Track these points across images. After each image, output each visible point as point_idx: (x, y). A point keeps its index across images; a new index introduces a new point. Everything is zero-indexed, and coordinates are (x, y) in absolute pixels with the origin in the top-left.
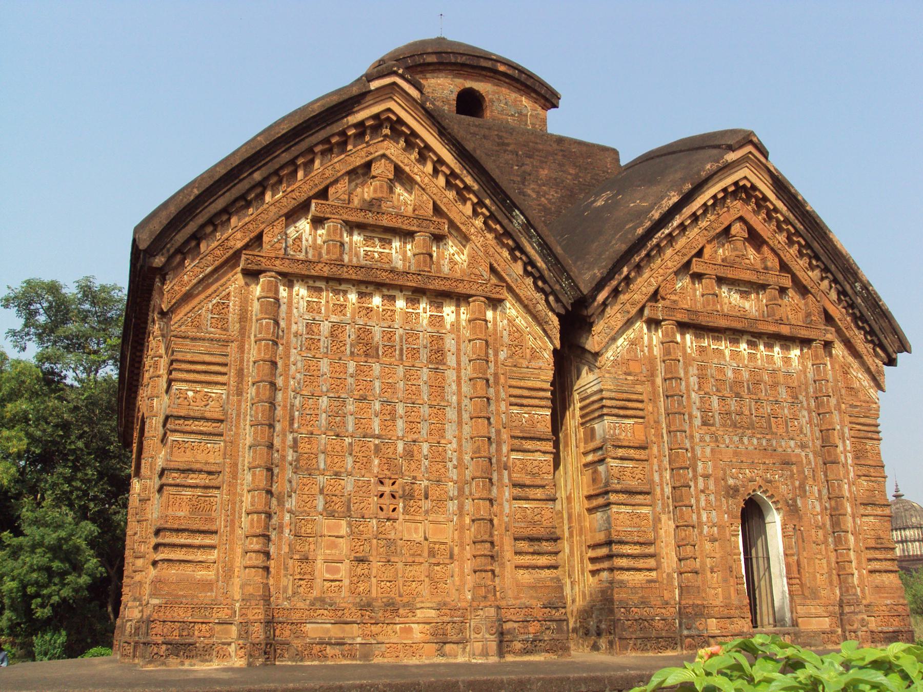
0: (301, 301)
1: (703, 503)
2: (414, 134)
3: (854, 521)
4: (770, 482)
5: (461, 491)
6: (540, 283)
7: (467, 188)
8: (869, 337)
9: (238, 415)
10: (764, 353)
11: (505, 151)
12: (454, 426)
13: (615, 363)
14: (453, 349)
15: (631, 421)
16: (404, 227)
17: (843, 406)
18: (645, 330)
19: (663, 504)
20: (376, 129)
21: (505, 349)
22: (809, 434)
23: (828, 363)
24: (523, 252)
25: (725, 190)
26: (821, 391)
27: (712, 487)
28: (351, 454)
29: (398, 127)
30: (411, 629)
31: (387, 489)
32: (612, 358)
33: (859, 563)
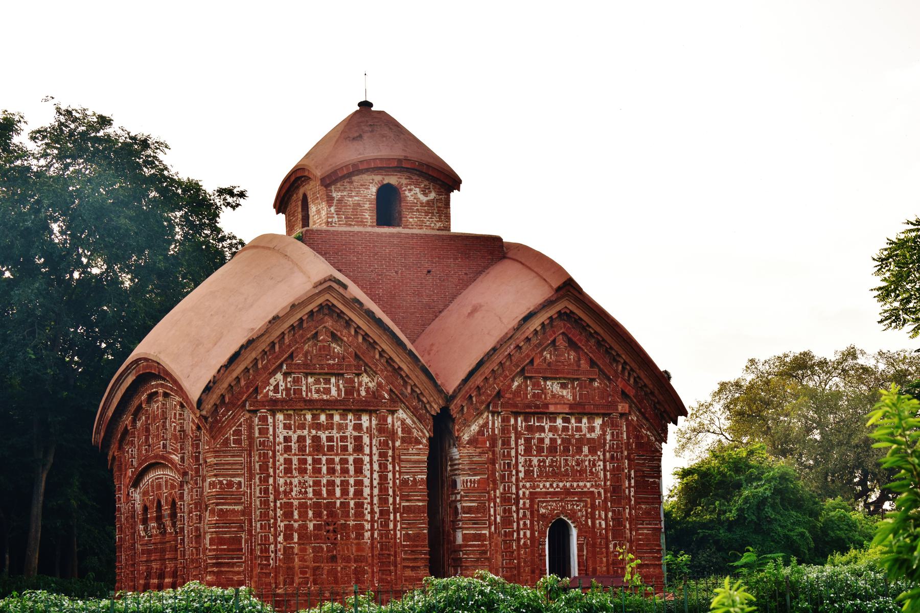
1: (521, 526)
5: (372, 526)
14: (368, 443)
18: (490, 418)
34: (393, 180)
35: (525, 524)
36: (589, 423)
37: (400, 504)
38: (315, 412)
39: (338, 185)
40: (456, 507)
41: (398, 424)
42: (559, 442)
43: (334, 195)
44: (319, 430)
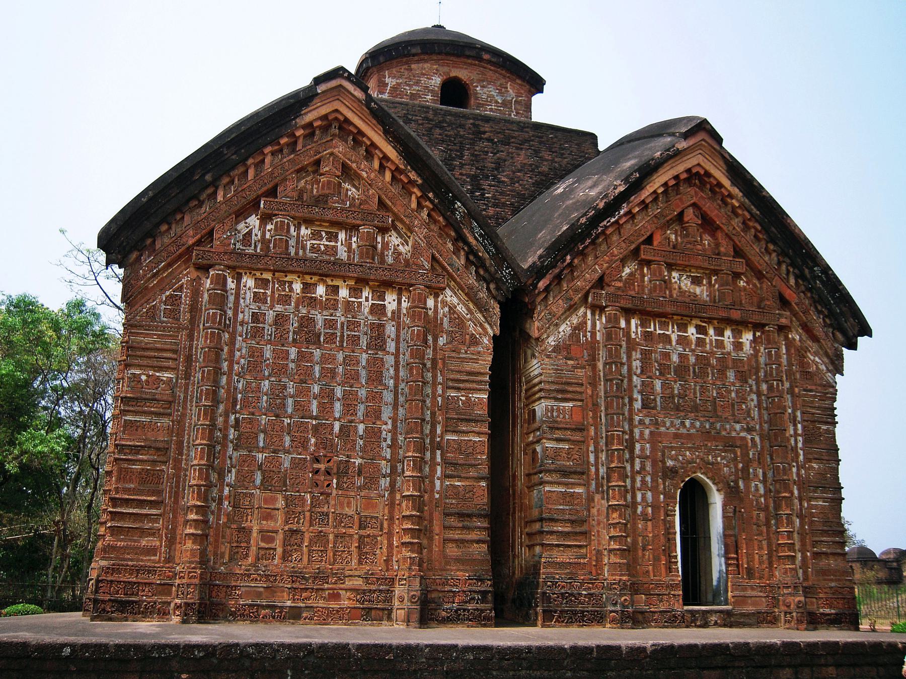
0: (248, 292)
1: (638, 484)
2: (361, 133)
3: (801, 504)
4: (712, 464)
5: (393, 468)
6: (482, 272)
7: (412, 182)
8: (828, 321)
9: (185, 398)
10: (714, 338)
11: (481, 139)
12: (390, 407)
13: (557, 349)
14: (393, 336)
15: (570, 404)
16: (349, 221)
17: (796, 390)
19: (596, 484)
20: (325, 129)
21: (445, 336)
22: (756, 417)
23: (784, 347)
24: (466, 242)
25: (676, 177)
26: (771, 374)
27: (649, 468)
28: (288, 434)
29: (345, 126)
30: (338, 595)
31: (322, 467)
32: (553, 343)
33: (803, 544)
34: (462, 73)
35: (643, 482)
36: (734, 337)
37: (442, 437)
38: (307, 277)
39: (394, 71)
40: (534, 451)
41: (443, 311)
42: (692, 360)
43: (387, 80)
44: (314, 308)
